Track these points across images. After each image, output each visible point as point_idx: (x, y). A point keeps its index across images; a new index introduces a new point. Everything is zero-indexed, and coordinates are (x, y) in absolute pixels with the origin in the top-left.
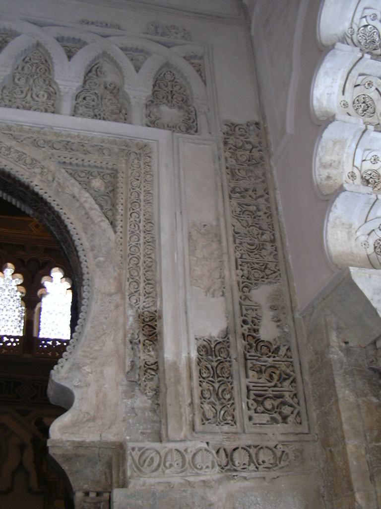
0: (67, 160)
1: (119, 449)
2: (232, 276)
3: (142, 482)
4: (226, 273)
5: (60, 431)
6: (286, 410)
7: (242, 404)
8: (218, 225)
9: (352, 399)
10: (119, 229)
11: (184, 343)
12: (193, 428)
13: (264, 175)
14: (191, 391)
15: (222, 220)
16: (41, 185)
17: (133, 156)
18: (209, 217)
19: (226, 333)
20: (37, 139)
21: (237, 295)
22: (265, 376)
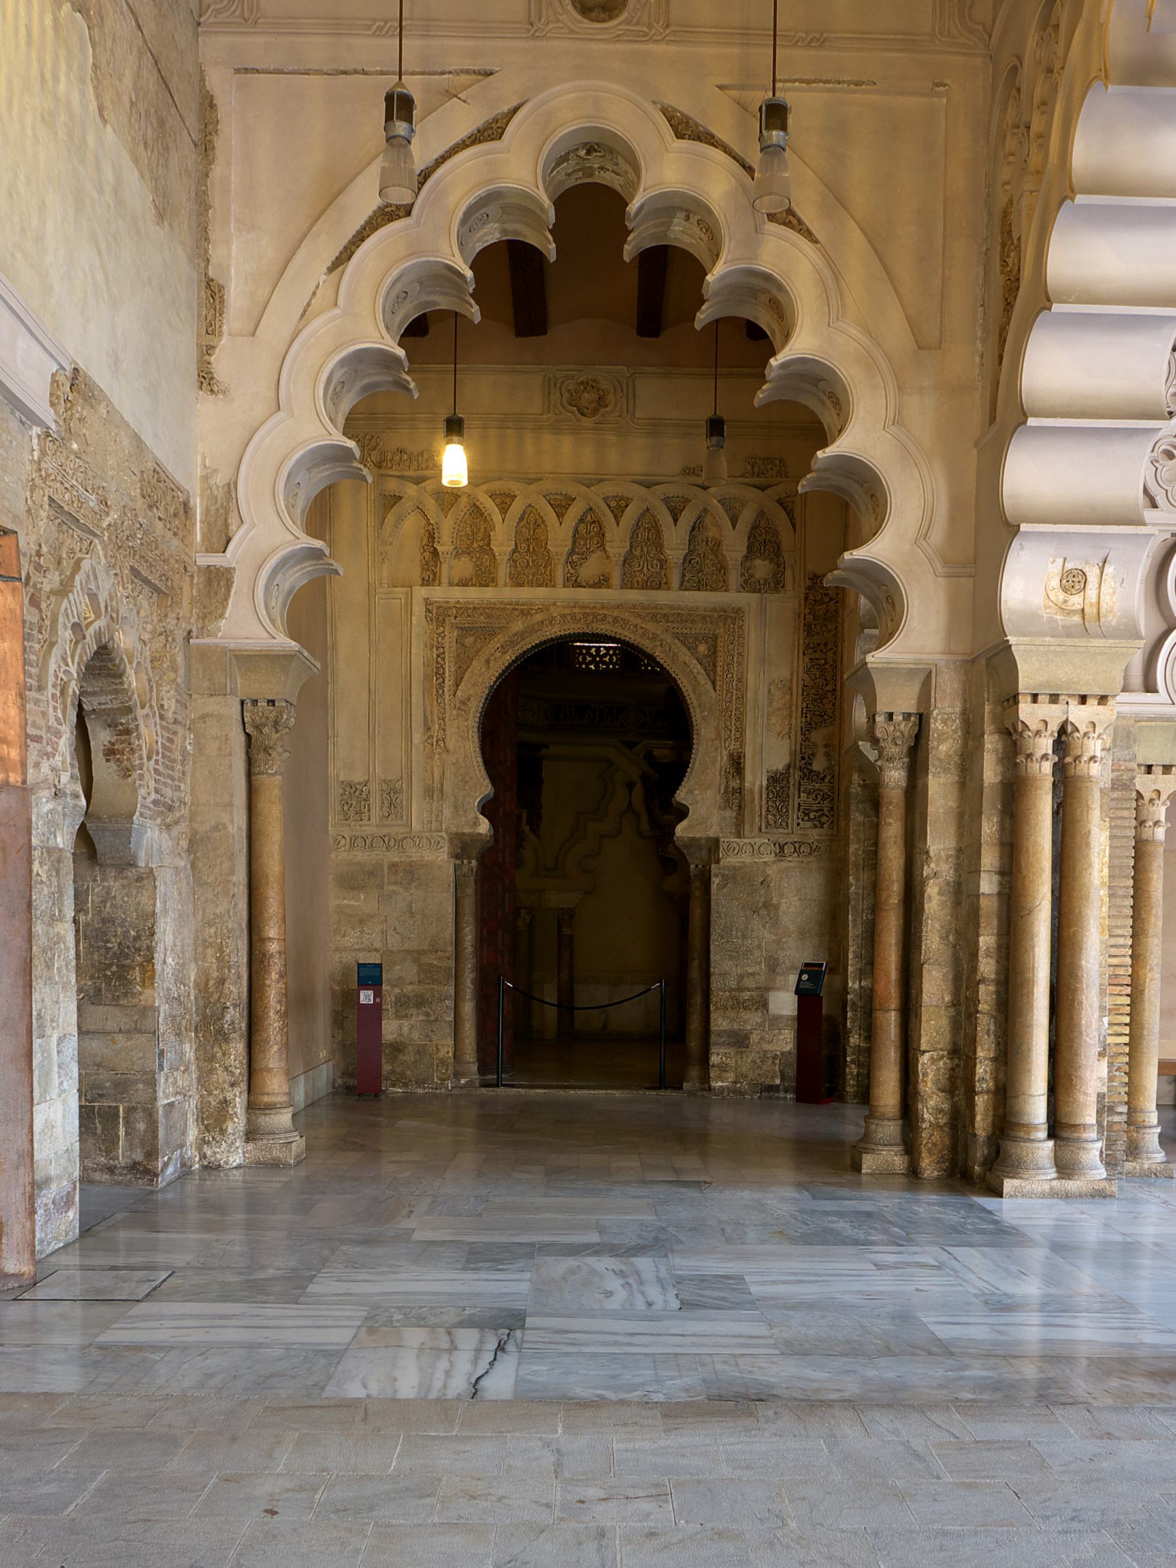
0: (679, 631)
1: (717, 840)
2: (798, 722)
3: (729, 860)
4: (794, 721)
5: (681, 830)
6: (824, 819)
7: (794, 816)
8: (791, 680)
9: (861, 818)
10: (718, 688)
11: (759, 775)
12: (760, 830)
13: (836, 628)
14: (761, 807)
15: (795, 675)
16: (662, 655)
17: (729, 621)
18: (784, 672)
19: (788, 767)
20: (656, 614)
21: (799, 737)
22: (813, 796)
